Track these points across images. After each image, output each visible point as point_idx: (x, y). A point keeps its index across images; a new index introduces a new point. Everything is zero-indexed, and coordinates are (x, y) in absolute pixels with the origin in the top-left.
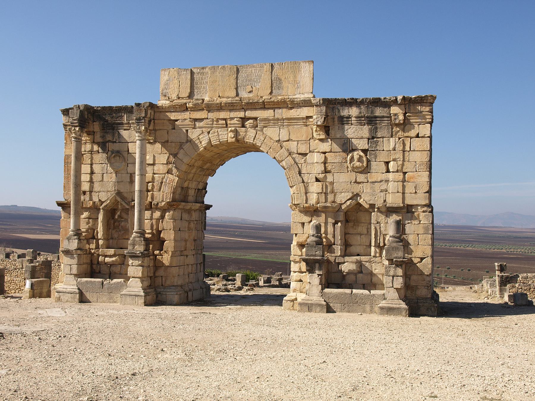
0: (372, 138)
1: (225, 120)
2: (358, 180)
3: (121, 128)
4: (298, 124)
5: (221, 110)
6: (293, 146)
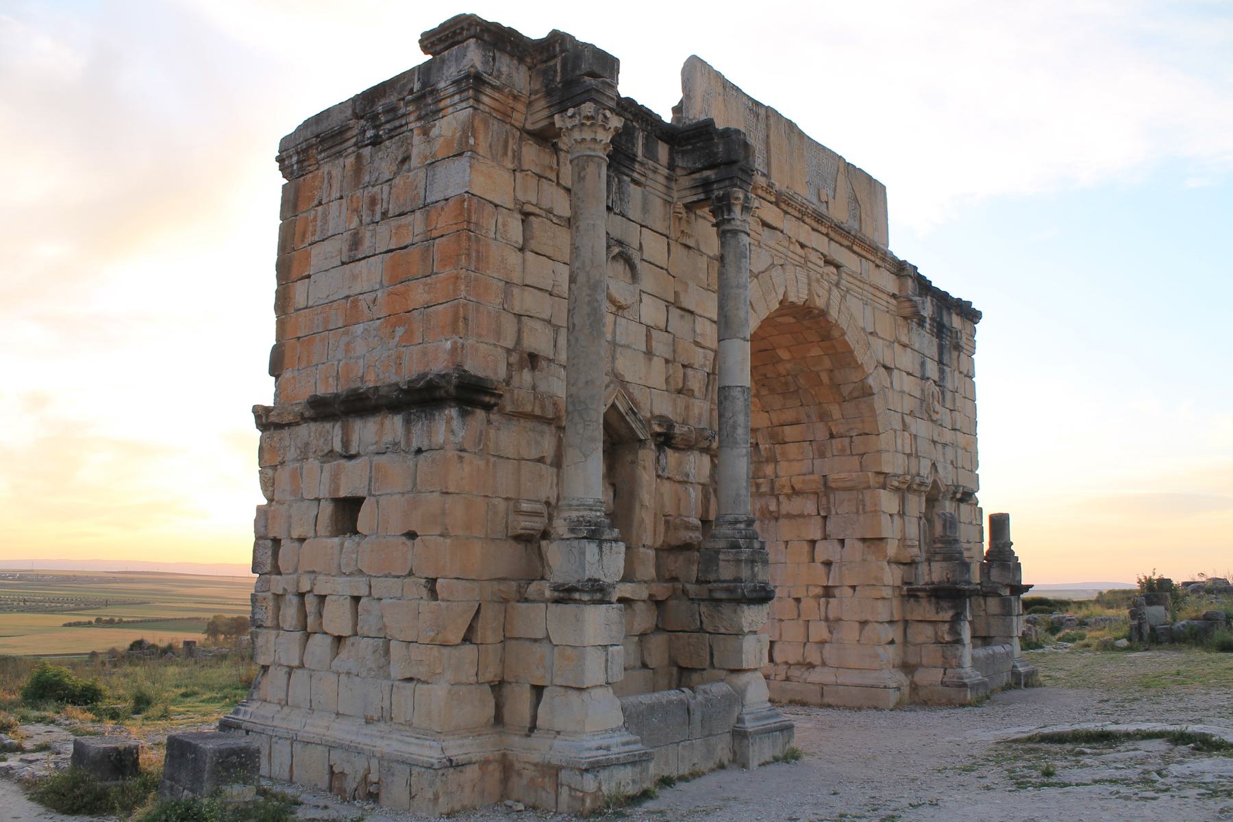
0: (940, 362)
1: (802, 246)
2: (935, 439)
3: (626, 171)
4: (881, 301)
5: (801, 223)
6: (880, 350)
